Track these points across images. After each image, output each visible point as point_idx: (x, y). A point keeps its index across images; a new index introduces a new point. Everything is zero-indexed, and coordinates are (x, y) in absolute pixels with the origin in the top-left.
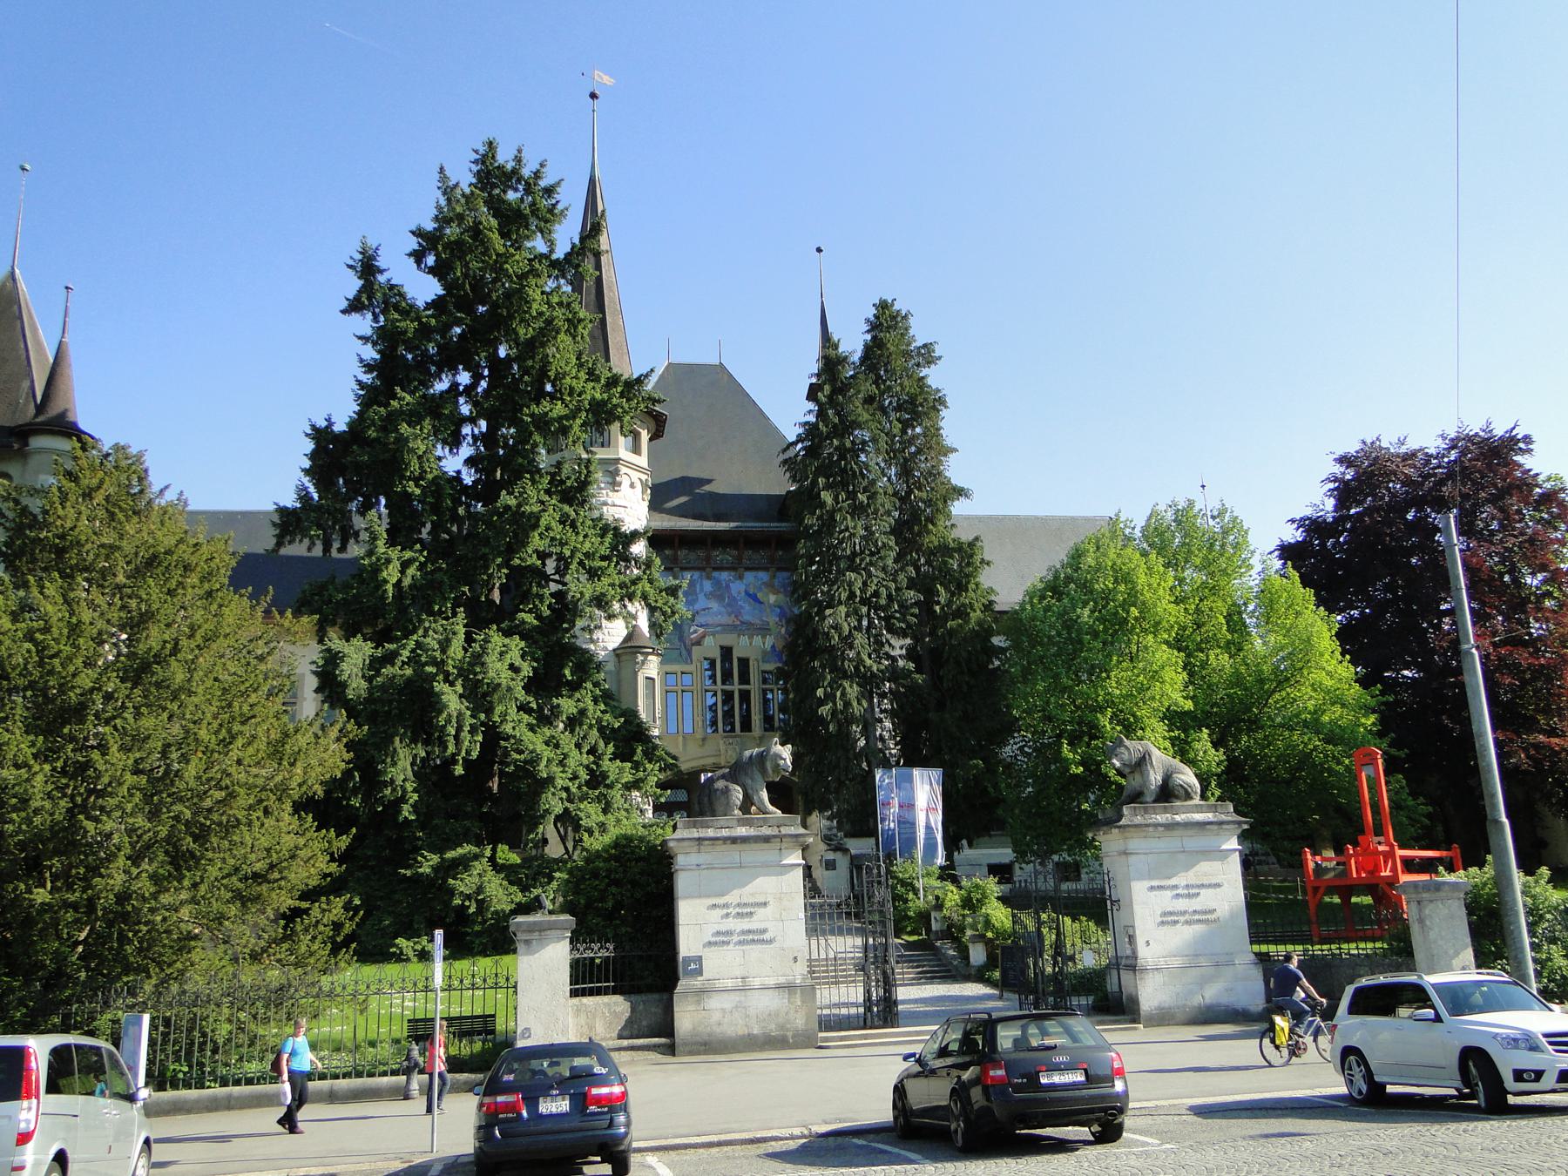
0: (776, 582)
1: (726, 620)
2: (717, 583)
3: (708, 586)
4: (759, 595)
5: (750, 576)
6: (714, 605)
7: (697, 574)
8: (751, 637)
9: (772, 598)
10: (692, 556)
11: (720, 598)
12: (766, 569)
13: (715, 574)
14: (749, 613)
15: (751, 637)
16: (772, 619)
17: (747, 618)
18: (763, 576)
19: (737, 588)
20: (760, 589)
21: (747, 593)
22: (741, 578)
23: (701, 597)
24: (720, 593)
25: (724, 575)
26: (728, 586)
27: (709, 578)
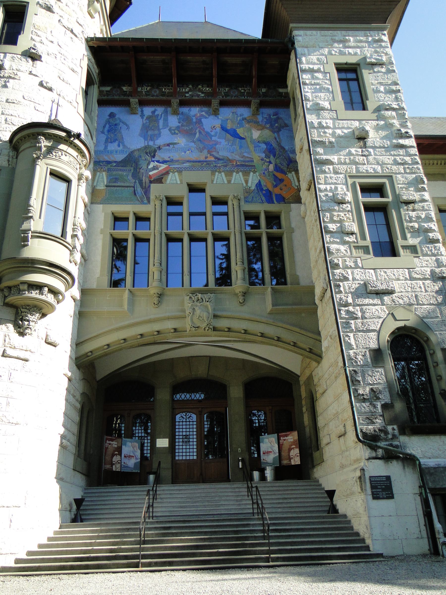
0: (260, 118)
1: (195, 156)
2: (187, 119)
3: (173, 121)
4: (240, 131)
5: (227, 113)
6: (181, 141)
7: (160, 110)
8: (229, 174)
9: (256, 134)
10: (156, 92)
11: (189, 134)
12: (247, 104)
13: (184, 110)
14: (225, 148)
15: (229, 174)
16: (257, 156)
17: (222, 154)
18: (244, 112)
19: (211, 123)
20: (240, 124)
21: (223, 128)
22: (216, 113)
23: (165, 132)
24: (188, 129)
25: (195, 111)
26: (199, 122)
27: (175, 113)
